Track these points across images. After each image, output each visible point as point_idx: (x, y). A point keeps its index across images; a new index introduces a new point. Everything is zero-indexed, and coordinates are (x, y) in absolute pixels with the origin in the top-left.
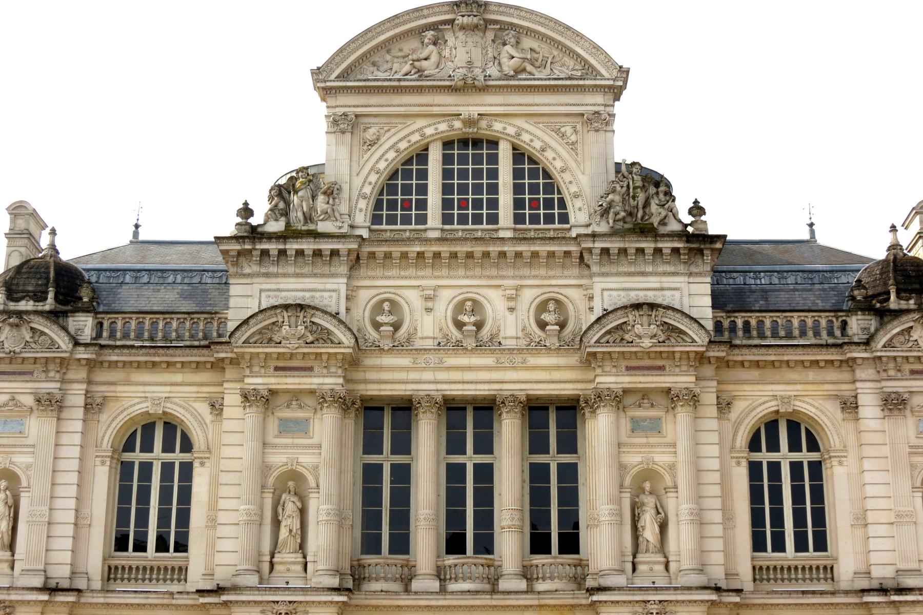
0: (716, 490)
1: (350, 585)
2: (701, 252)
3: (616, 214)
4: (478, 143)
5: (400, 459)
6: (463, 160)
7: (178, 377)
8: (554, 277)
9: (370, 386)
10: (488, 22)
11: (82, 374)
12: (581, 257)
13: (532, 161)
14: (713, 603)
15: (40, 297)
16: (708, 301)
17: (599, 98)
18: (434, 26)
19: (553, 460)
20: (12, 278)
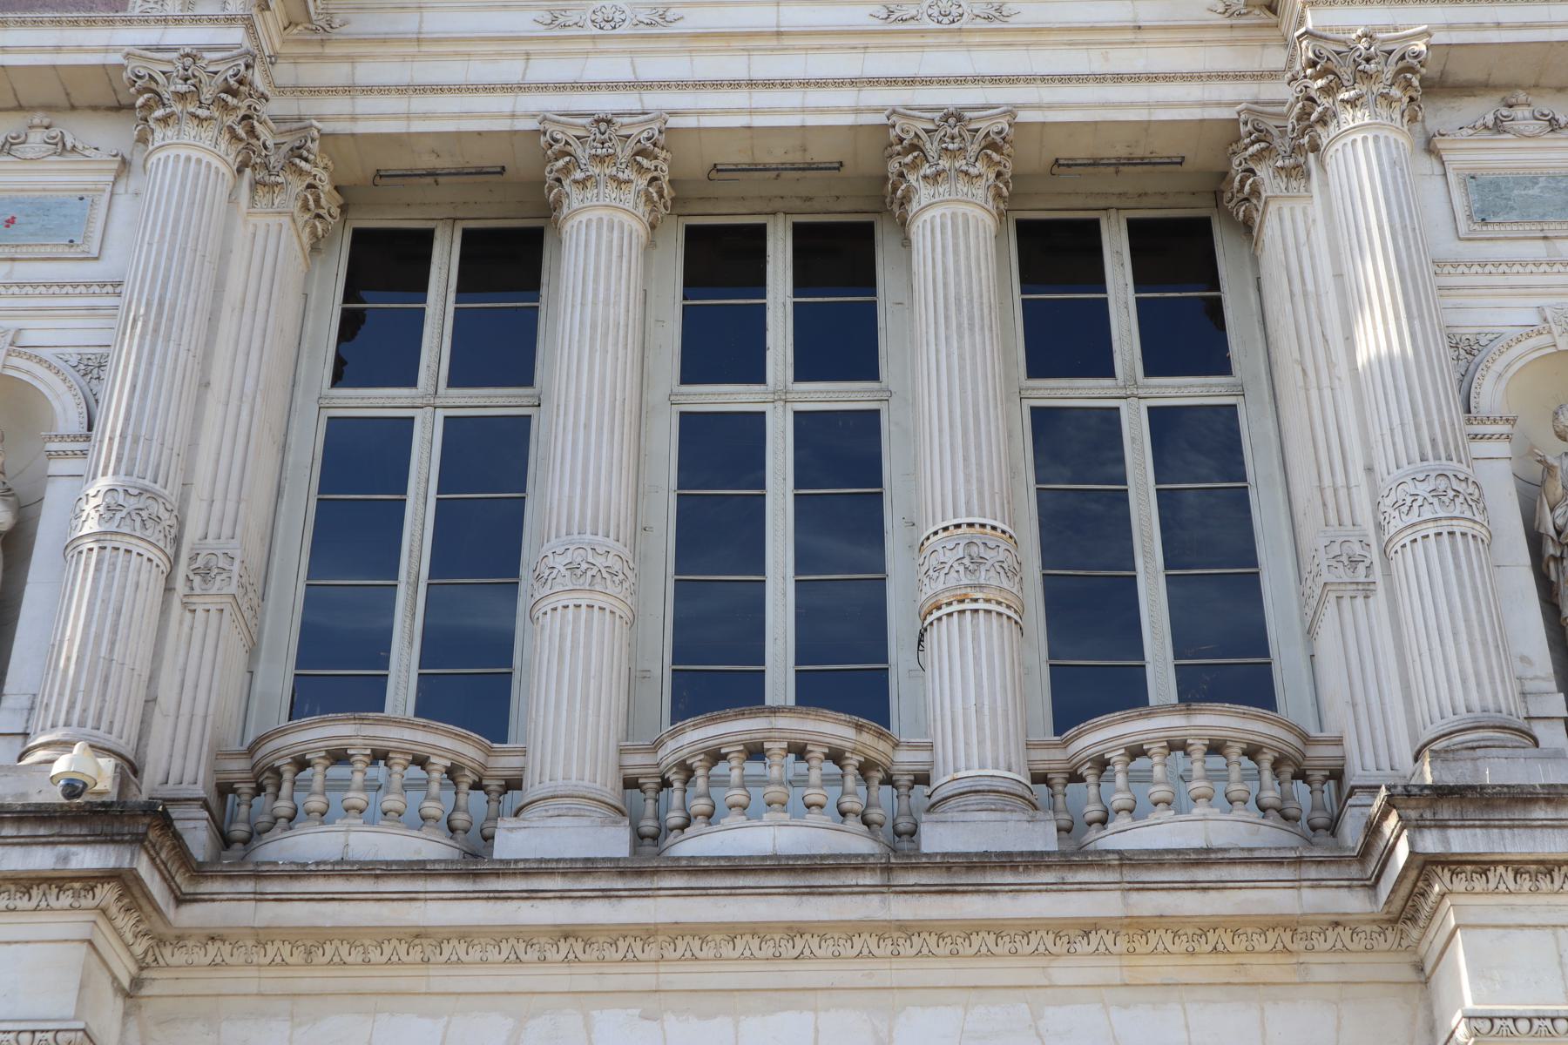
9: (365, 104)
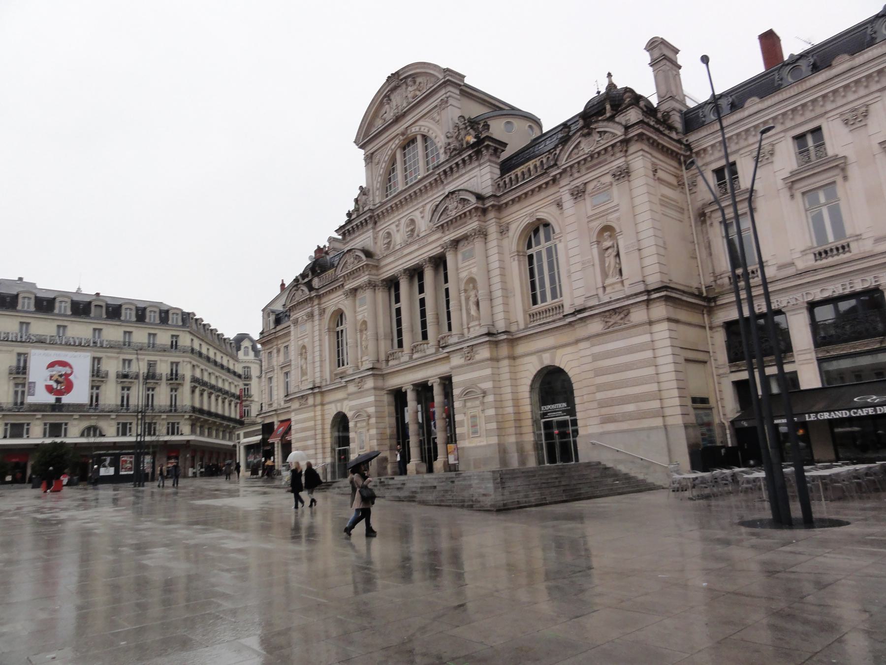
18: (385, 96)
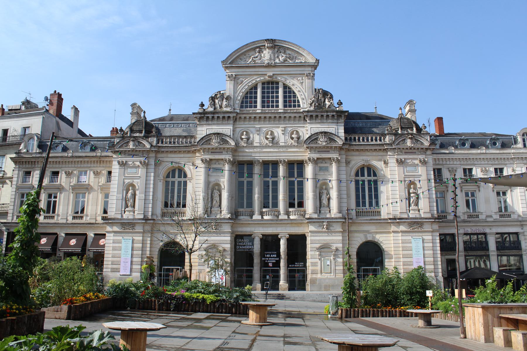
0: (345, 188)
1: (234, 217)
2: (341, 116)
3: (315, 104)
4: (272, 83)
5: (250, 179)
6: (268, 88)
7: (182, 155)
8: (296, 124)
10: (275, 45)
11: (153, 155)
12: (304, 118)
13: (289, 88)
14: (344, 222)
15: (140, 132)
16: (343, 131)
17: (310, 69)
19: (296, 180)
20: (132, 126)
